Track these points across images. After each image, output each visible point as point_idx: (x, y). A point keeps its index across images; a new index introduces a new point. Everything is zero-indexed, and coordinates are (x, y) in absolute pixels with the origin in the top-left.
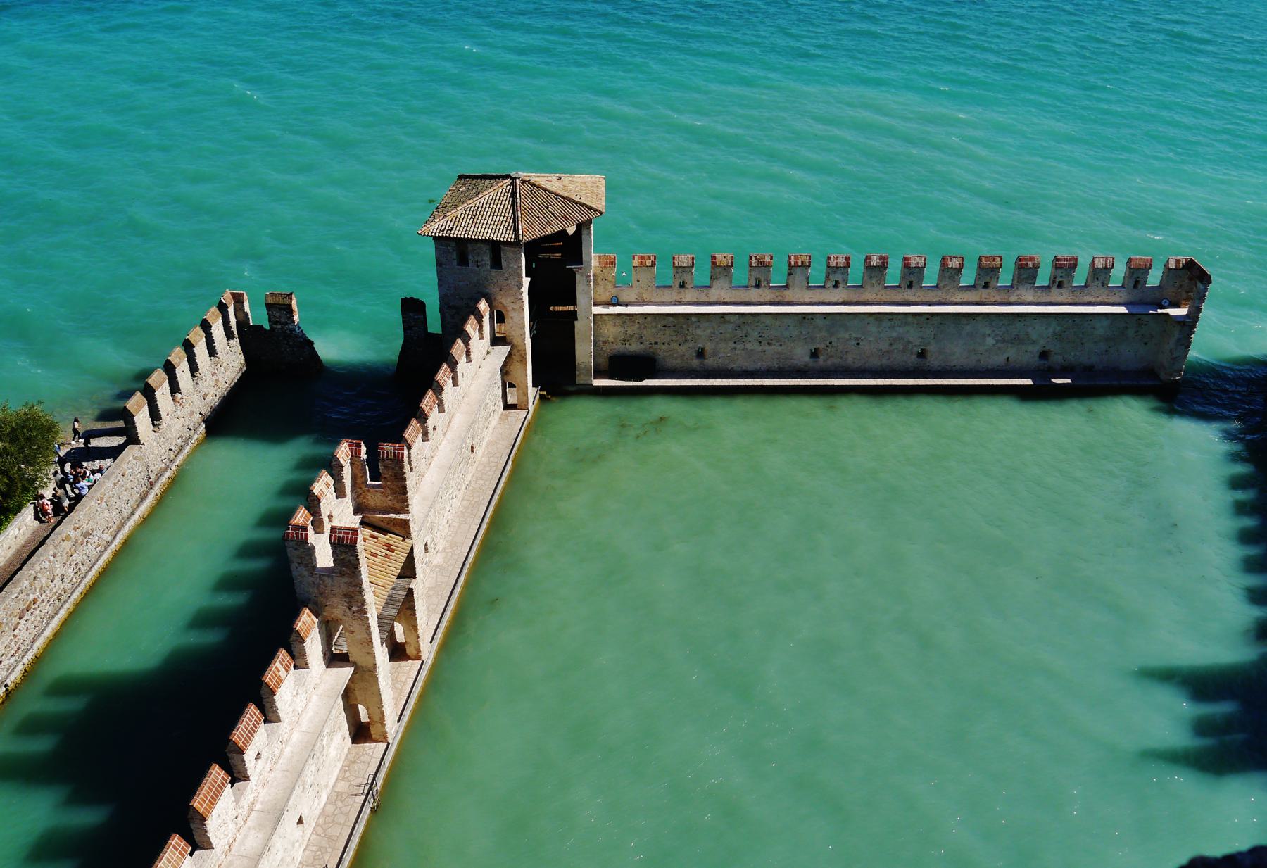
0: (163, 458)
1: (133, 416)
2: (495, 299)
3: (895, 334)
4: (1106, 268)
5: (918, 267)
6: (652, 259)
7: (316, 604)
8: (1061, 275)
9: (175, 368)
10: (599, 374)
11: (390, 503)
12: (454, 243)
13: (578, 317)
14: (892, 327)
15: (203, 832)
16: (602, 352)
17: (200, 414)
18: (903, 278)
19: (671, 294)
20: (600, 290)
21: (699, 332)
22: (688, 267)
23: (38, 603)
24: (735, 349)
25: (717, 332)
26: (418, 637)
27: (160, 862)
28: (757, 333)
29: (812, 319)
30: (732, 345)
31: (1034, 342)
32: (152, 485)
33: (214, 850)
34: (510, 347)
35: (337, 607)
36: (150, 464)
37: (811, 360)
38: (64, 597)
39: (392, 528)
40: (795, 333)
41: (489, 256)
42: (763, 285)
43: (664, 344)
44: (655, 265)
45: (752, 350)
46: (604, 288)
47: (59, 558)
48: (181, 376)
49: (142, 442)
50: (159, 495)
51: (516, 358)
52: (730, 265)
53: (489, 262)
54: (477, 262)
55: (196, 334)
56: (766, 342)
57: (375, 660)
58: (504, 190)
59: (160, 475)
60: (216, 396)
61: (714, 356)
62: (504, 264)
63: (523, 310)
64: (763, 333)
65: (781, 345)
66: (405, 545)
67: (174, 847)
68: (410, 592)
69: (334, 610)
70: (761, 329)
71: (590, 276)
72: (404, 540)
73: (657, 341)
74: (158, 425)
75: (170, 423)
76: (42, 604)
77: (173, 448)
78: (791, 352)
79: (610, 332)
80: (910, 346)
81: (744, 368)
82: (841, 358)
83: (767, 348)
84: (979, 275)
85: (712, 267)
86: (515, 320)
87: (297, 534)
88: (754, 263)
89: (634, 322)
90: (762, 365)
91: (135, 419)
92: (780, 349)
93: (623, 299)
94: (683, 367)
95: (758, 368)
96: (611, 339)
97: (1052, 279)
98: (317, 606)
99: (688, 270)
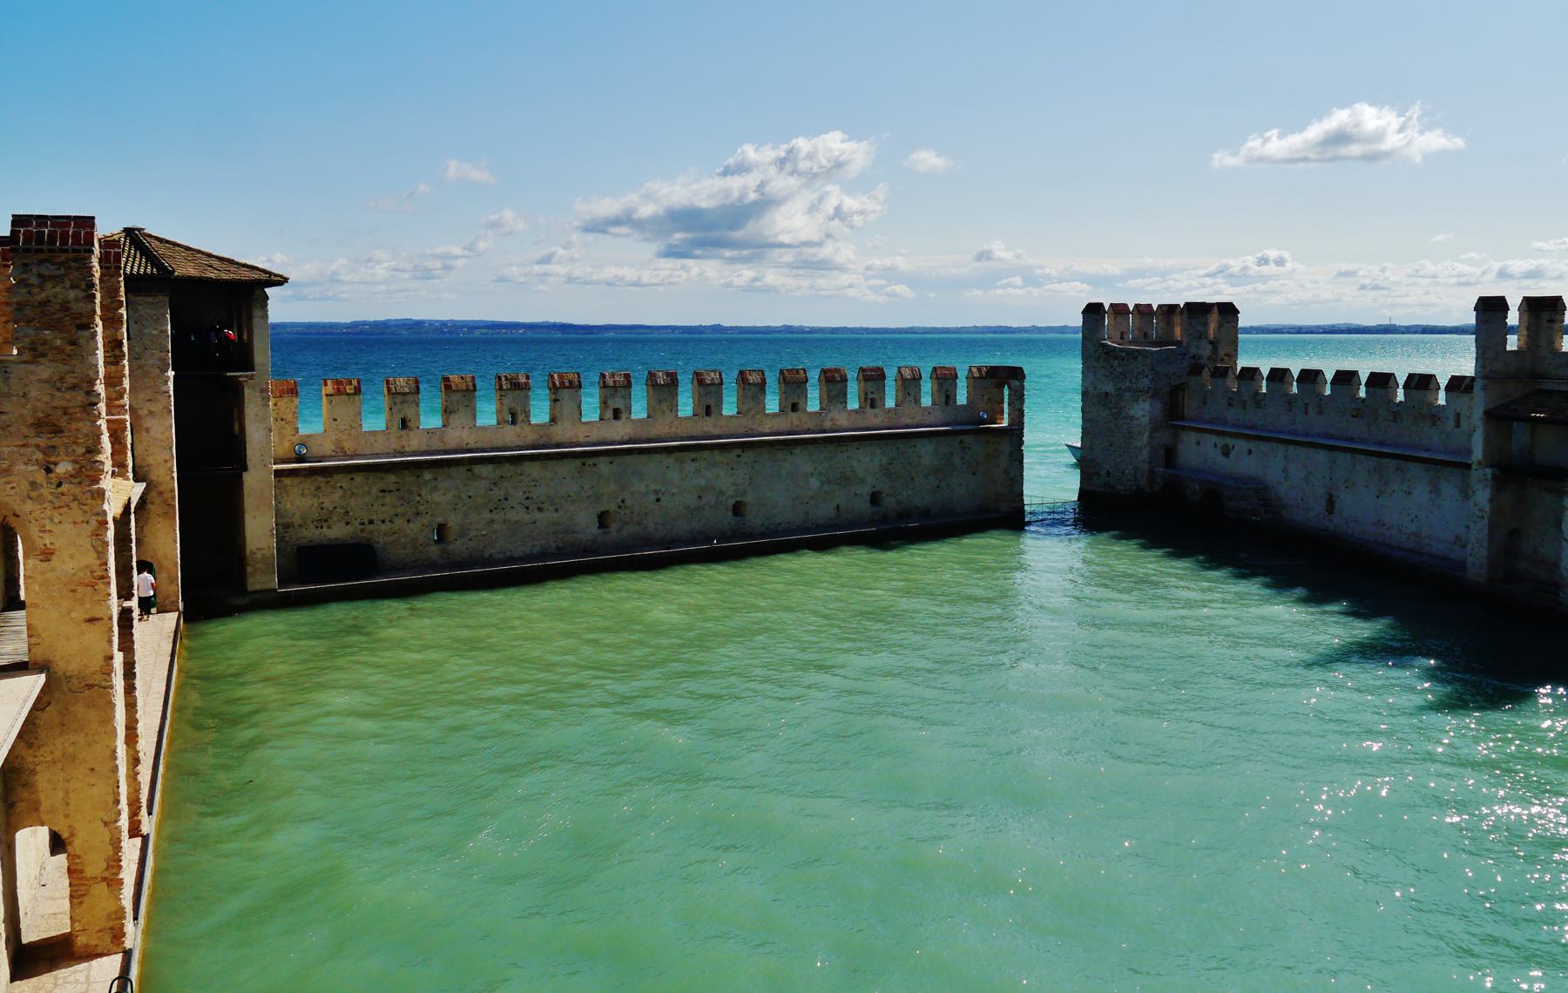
3: (702, 482)
4: (914, 379)
5: (715, 384)
6: (355, 383)
8: (873, 390)
13: (249, 463)
14: (698, 471)
19: (388, 439)
21: (437, 497)
22: (408, 393)
24: (492, 521)
25: (463, 495)
28: (521, 493)
29: (595, 465)
30: (486, 515)
31: (862, 481)
34: (145, 484)
42: (520, 419)
43: (383, 522)
44: (360, 391)
45: (517, 522)
46: (280, 433)
51: (154, 508)
52: (472, 388)
64: (529, 492)
65: (557, 510)
70: (527, 486)
79: (301, 501)
81: (508, 554)
82: (639, 524)
83: (538, 515)
84: (785, 392)
86: (152, 433)
88: (505, 385)
89: (334, 487)
92: (555, 515)
93: (316, 450)
94: (416, 561)
96: (297, 520)
97: (863, 397)
99: (410, 398)
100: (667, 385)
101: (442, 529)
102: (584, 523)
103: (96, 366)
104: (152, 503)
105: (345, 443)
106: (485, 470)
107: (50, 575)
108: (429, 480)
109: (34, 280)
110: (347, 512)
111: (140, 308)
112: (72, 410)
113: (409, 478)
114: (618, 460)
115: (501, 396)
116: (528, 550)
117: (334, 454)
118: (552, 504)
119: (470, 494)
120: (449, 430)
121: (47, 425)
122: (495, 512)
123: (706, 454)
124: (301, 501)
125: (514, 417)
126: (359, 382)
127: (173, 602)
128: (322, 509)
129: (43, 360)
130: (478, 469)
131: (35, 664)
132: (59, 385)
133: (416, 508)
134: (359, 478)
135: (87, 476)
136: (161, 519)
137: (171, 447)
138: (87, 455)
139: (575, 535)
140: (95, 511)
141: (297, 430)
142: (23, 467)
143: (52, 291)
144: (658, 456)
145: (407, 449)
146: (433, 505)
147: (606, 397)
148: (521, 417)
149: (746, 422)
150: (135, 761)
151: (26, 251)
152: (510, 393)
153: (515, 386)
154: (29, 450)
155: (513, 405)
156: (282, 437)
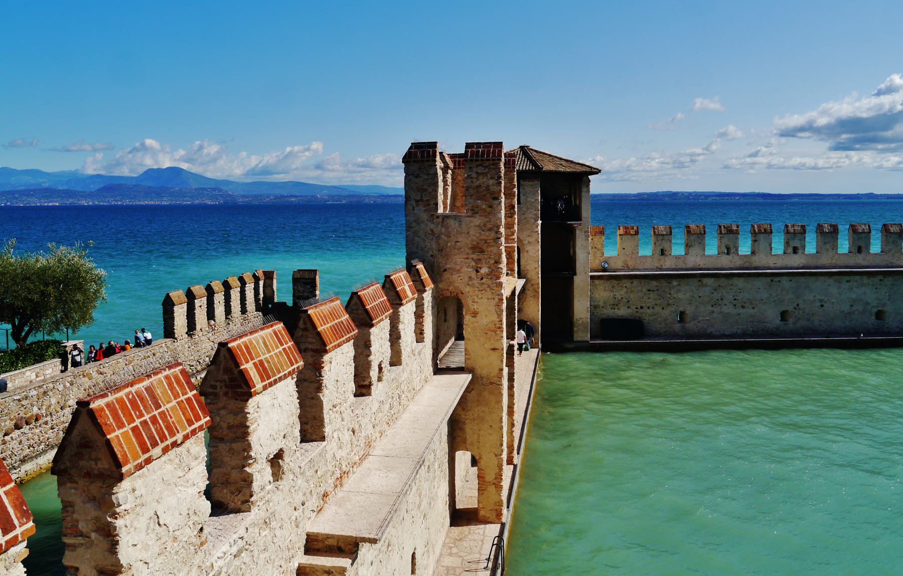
0: (192, 364)
1: (174, 305)
3: (854, 296)
6: (635, 228)
14: (851, 289)
18: (853, 243)
19: (653, 261)
21: (680, 296)
23: (41, 421)
24: (713, 312)
25: (696, 296)
30: (709, 308)
33: (324, 443)
37: (782, 323)
42: (732, 252)
45: (728, 313)
46: (594, 255)
49: (176, 336)
51: (529, 293)
52: (703, 232)
55: (234, 280)
61: (694, 320)
64: (737, 296)
65: (753, 308)
69: (455, 277)
73: (642, 305)
79: (603, 293)
80: (869, 307)
81: (722, 332)
82: (808, 320)
83: (741, 311)
91: (175, 308)
92: (752, 311)
93: (613, 265)
96: (601, 304)
99: (666, 237)
100: (831, 232)
101: (682, 314)
102: (772, 317)
103: (501, 218)
104: (528, 290)
105: (629, 262)
106: (709, 281)
107: (476, 324)
112: (488, 241)
113: (664, 283)
114: (794, 279)
115: (721, 237)
118: (751, 303)
120: (688, 256)
121: (477, 249)
122: (714, 306)
123: (857, 278)
124: (603, 293)
125: (729, 250)
126: (637, 228)
128: (615, 298)
131: (468, 369)
132: (483, 228)
133: (668, 301)
134: (636, 282)
135: (494, 275)
136: (532, 299)
137: (538, 261)
138: (495, 264)
140: (498, 293)
142: (466, 269)
143: (482, 180)
144: (822, 278)
145: (664, 267)
147: (788, 239)
148: (733, 250)
149: (887, 259)
150: (512, 425)
151: (471, 160)
154: (469, 261)
155: (728, 243)
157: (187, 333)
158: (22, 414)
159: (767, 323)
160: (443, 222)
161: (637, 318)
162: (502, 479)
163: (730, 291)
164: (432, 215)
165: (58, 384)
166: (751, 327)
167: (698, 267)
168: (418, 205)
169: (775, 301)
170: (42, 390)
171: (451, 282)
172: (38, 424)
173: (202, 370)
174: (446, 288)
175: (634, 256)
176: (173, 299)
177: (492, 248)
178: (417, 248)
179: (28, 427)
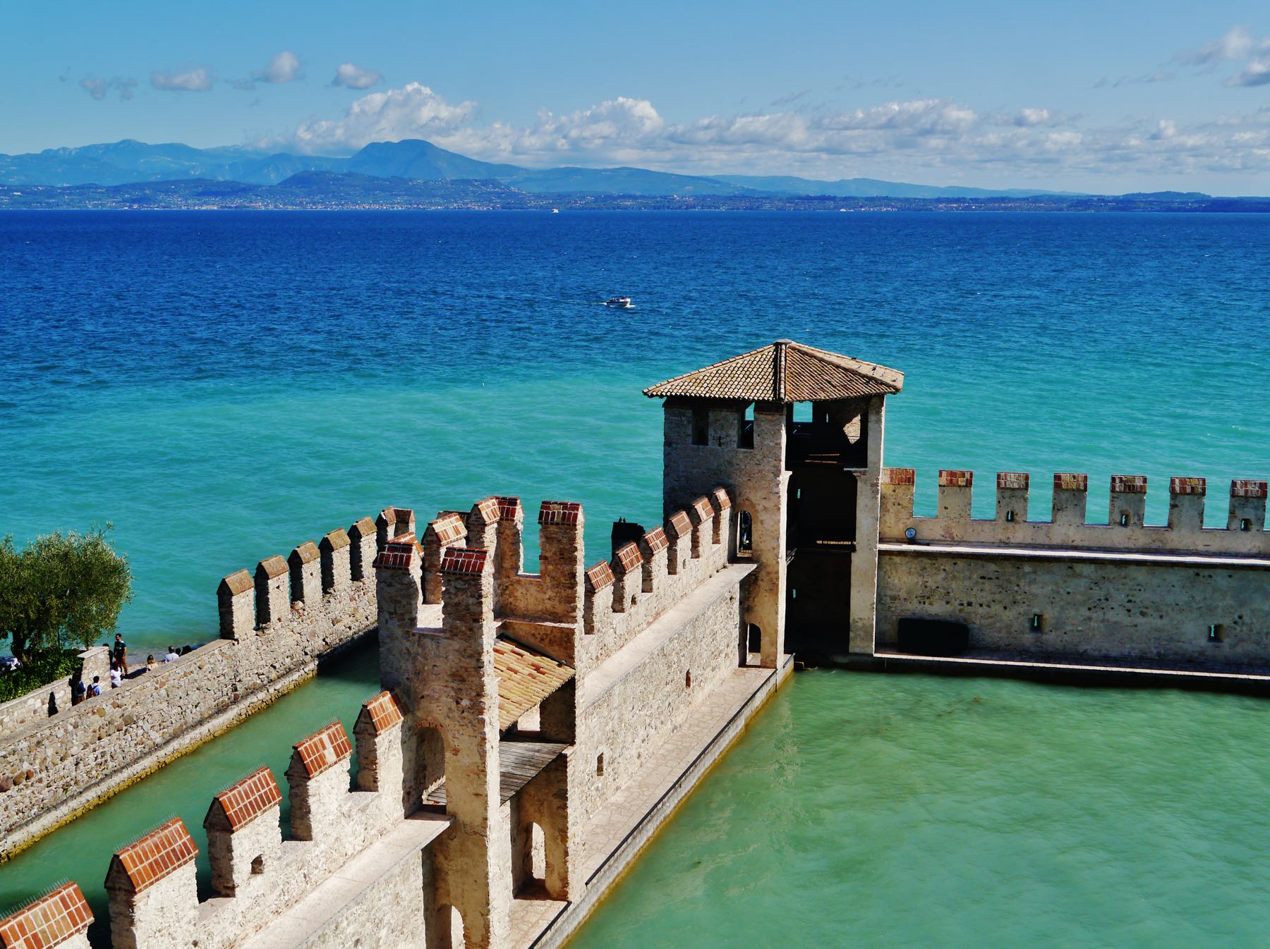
0: (261, 672)
1: (231, 595)
2: (740, 494)
6: (967, 476)
7: (407, 692)
9: (302, 563)
10: (880, 646)
11: (548, 605)
12: (691, 411)
15: (127, 921)
16: (889, 614)
17: (324, 640)
19: (994, 530)
20: (890, 518)
21: (1035, 589)
23: (33, 780)
24: (1090, 619)
25: (1062, 591)
26: (566, 854)
27: (29, 910)
29: (1210, 576)
30: (1084, 612)
32: (236, 701)
35: (438, 700)
36: (241, 671)
37: (1211, 644)
38: (73, 789)
39: (547, 648)
40: (1185, 598)
41: (736, 429)
42: (1132, 522)
43: (981, 605)
44: (971, 484)
45: (1116, 623)
46: (896, 516)
47: (80, 733)
48: (307, 578)
49: (236, 636)
50: (244, 716)
51: (764, 585)
53: (736, 439)
54: (720, 438)
55: (339, 536)
56: (1138, 611)
57: (486, 810)
58: (764, 356)
59: (252, 691)
60: (350, 628)
61: (1056, 629)
62: (756, 440)
63: (779, 509)
64: (1133, 596)
65: (1161, 617)
66: (566, 673)
67: (63, 899)
68: (561, 761)
69: (434, 706)
70: (1130, 589)
71: (877, 485)
72: (560, 665)
74: (263, 629)
75: (280, 632)
76: (38, 784)
77: (277, 665)
78: (1177, 629)
79: (904, 580)
81: (1104, 652)
82: (1258, 643)
83: (1140, 620)
85: (1055, 492)
86: (765, 525)
87: (395, 556)
90: (1132, 648)
91: (234, 599)
92: (1159, 622)
93: (925, 533)
94: (1009, 645)
95: (1126, 653)
96: (903, 594)
98: (409, 697)
99: (1019, 493)
102: (1193, 634)
104: (762, 580)
105: (953, 530)
108: (1029, 573)
109: (452, 590)
110: (948, 593)
111: (762, 424)
113: (1009, 568)
114: (1238, 575)
115: (1113, 497)
116: (1126, 652)
117: (942, 538)
118: (1157, 609)
119: (1069, 590)
120: (1055, 526)
122: (1093, 610)
127: (772, 660)
128: (926, 587)
129: (456, 638)
130: (1078, 568)
132: (463, 653)
133: (1014, 597)
134: (961, 564)
136: (767, 594)
139: (1181, 644)
141: (911, 515)
142: (445, 699)
145: (1012, 541)
146: (1030, 597)
147: (1234, 507)
152: (1124, 494)
153: (1129, 489)
155: (1125, 508)
156: (898, 520)
157: (256, 629)
158: (8, 774)
159: (1183, 642)
160: (419, 641)
161: (962, 620)
162: (489, 942)
163: (1120, 586)
164: (408, 632)
165: (57, 728)
166: (1156, 648)
167: (1070, 543)
168: (391, 618)
169: (1200, 608)
170: (35, 740)
171: (430, 712)
172: (30, 783)
173: (279, 678)
174: (424, 717)
175: (962, 520)
176: (231, 587)
177: (474, 679)
178: (392, 667)
179: (16, 788)
